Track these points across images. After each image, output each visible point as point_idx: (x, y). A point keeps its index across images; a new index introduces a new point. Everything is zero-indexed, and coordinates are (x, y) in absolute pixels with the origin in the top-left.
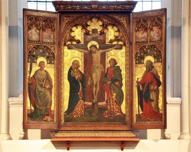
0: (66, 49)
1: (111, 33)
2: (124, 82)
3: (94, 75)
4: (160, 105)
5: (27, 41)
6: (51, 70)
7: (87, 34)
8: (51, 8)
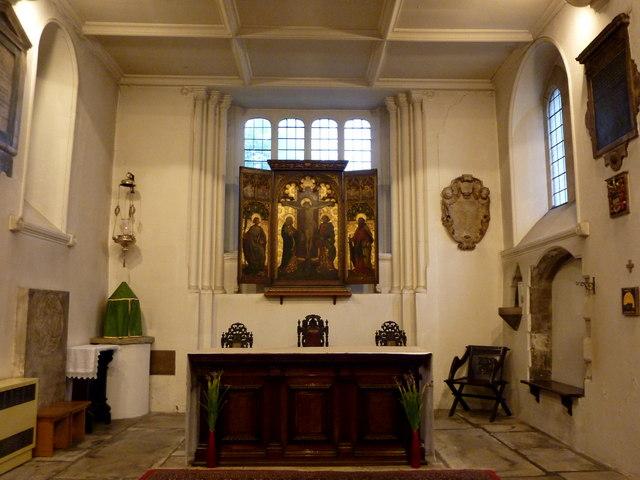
0: (280, 206)
1: (324, 190)
2: (336, 238)
3: (307, 231)
4: (373, 261)
5: (242, 197)
6: (265, 228)
7: (300, 191)
8: (267, 167)
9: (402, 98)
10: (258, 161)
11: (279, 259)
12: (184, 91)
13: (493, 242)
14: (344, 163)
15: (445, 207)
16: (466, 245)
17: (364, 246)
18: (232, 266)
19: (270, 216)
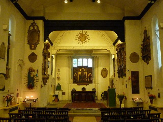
0: (79, 72)
1: (85, 70)
6: (77, 75)
9: (96, 57)
10: (75, 66)
11: (79, 79)
12: (66, 57)
13: (108, 77)
14: (88, 66)
15: (101, 72)
16: (104, 77)
17: (90, 77)
18: (72, 80)
19: (77, 73)
